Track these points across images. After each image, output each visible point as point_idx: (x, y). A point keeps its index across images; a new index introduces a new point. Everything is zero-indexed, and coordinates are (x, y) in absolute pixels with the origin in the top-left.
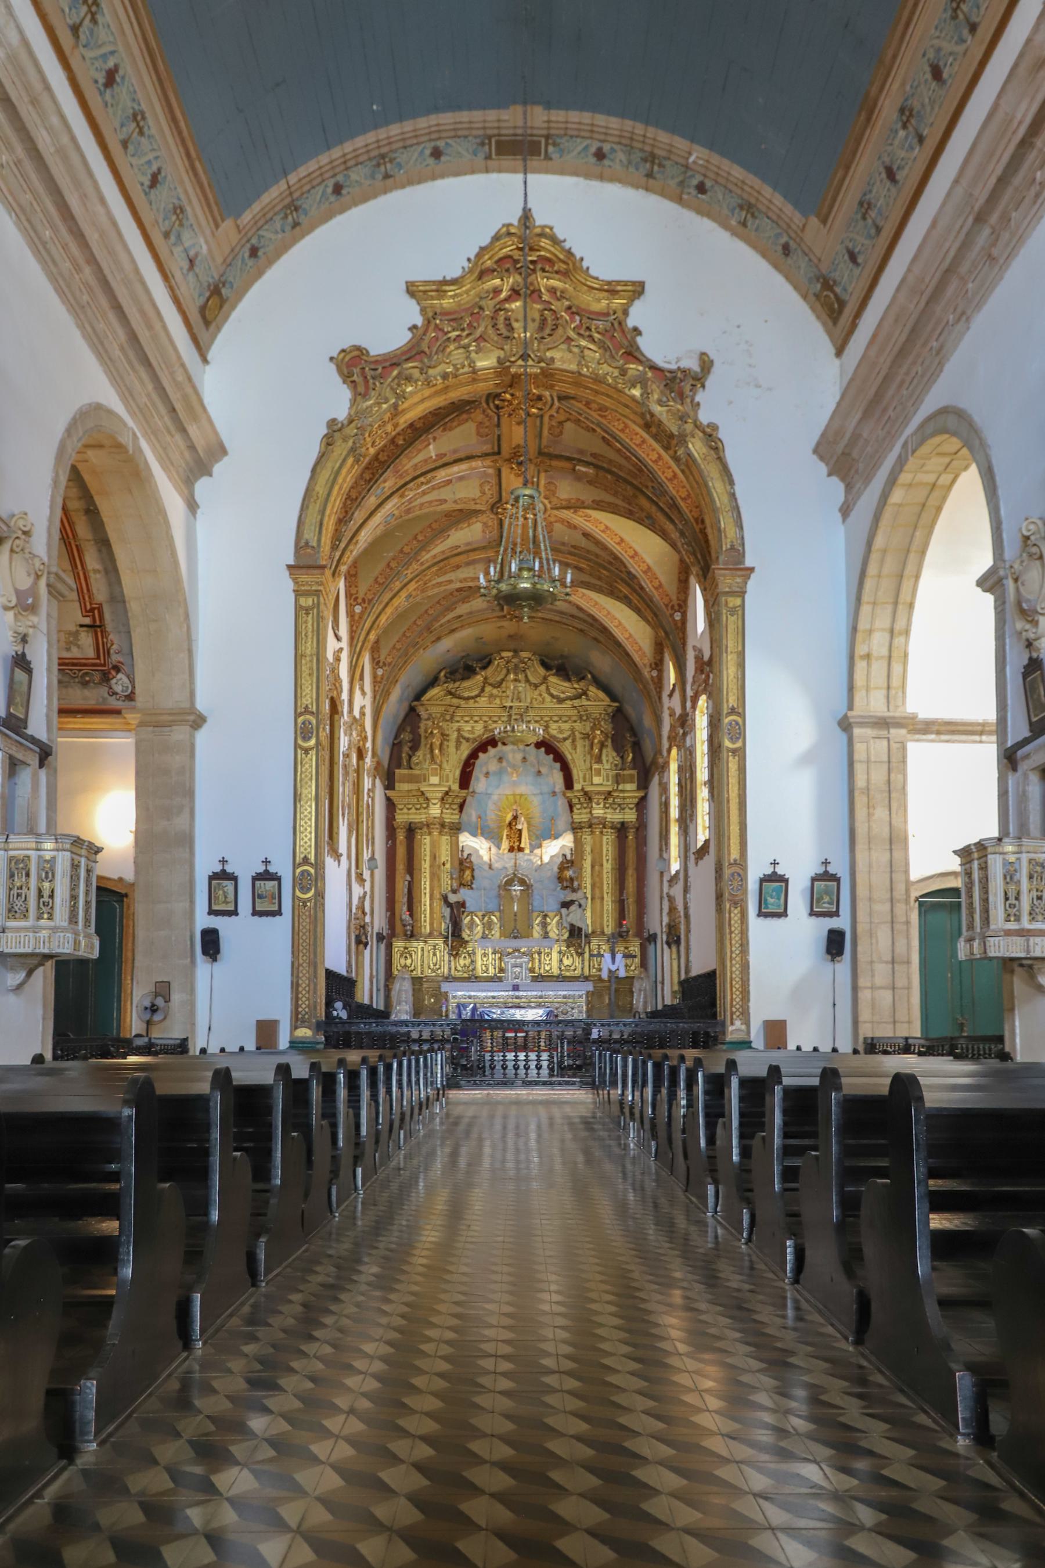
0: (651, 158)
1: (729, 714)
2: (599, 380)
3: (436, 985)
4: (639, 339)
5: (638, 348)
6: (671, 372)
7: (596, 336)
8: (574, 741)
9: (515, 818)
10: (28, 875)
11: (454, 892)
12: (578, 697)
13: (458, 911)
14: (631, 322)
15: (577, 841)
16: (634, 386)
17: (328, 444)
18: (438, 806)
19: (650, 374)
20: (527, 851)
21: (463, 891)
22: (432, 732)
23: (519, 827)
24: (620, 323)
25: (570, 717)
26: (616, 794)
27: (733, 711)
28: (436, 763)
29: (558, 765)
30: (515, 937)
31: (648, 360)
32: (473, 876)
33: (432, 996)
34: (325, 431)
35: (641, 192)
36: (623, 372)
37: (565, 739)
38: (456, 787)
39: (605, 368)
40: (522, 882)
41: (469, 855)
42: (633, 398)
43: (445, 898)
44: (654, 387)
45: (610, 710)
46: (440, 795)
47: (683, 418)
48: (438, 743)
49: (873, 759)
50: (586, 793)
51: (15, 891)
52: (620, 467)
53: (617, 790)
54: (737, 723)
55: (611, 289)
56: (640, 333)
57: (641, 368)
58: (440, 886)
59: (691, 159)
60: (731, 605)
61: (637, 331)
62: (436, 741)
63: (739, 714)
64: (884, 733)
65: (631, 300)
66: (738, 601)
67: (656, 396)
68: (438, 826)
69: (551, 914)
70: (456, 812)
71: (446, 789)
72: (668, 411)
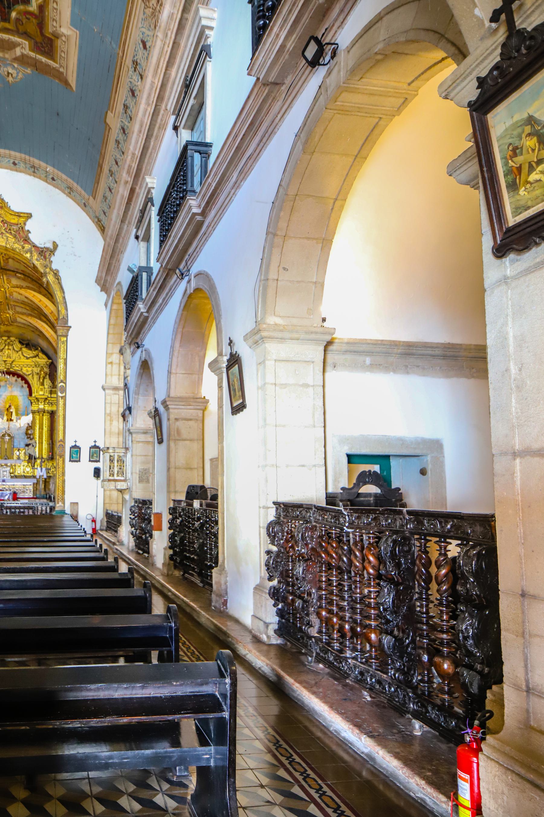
0: (33, 167)
1: (60, 383)
2: (13, 250)
4: (30, 235)
5: (29, 239)
6: (41, 248)
7: (13, 232)
8: (33, 375)
9: (10, 406)
12: (35, 357)
14: (27, 228)
15: (34, 418)
16: (27, 253)
19: (33, 249)
20: (15, 421)
23: (11, 410)
24: (22, 228)
25: (31, 365)
26: (49, 399)
27: (62, 381)
29: (26, 385)
30: (6, 459)
31: (33, 243)
35: (32, 177)
36: (23, 248)
37: (29, 375)
39: (16, 246)
40: (9, 435)
42: (27, 258)
44: (35, 254)
45: (48, 363)
47: (46, 267)
49: (113, 402)
50: (37, 398)
52: (33, 276)
53: (51, 397)
54: (63, 386)
55: (19, 215)
56: (30, 232)
57: (30, 246)
59: (48, 170)
60: (62, 340)
61: (29, 231)
63: (64, 383)
64: (117, 392)
65: (27, 220)
66: (65, 339)
67: (36, 257)
69: (21, 449)
72: (40, 263)
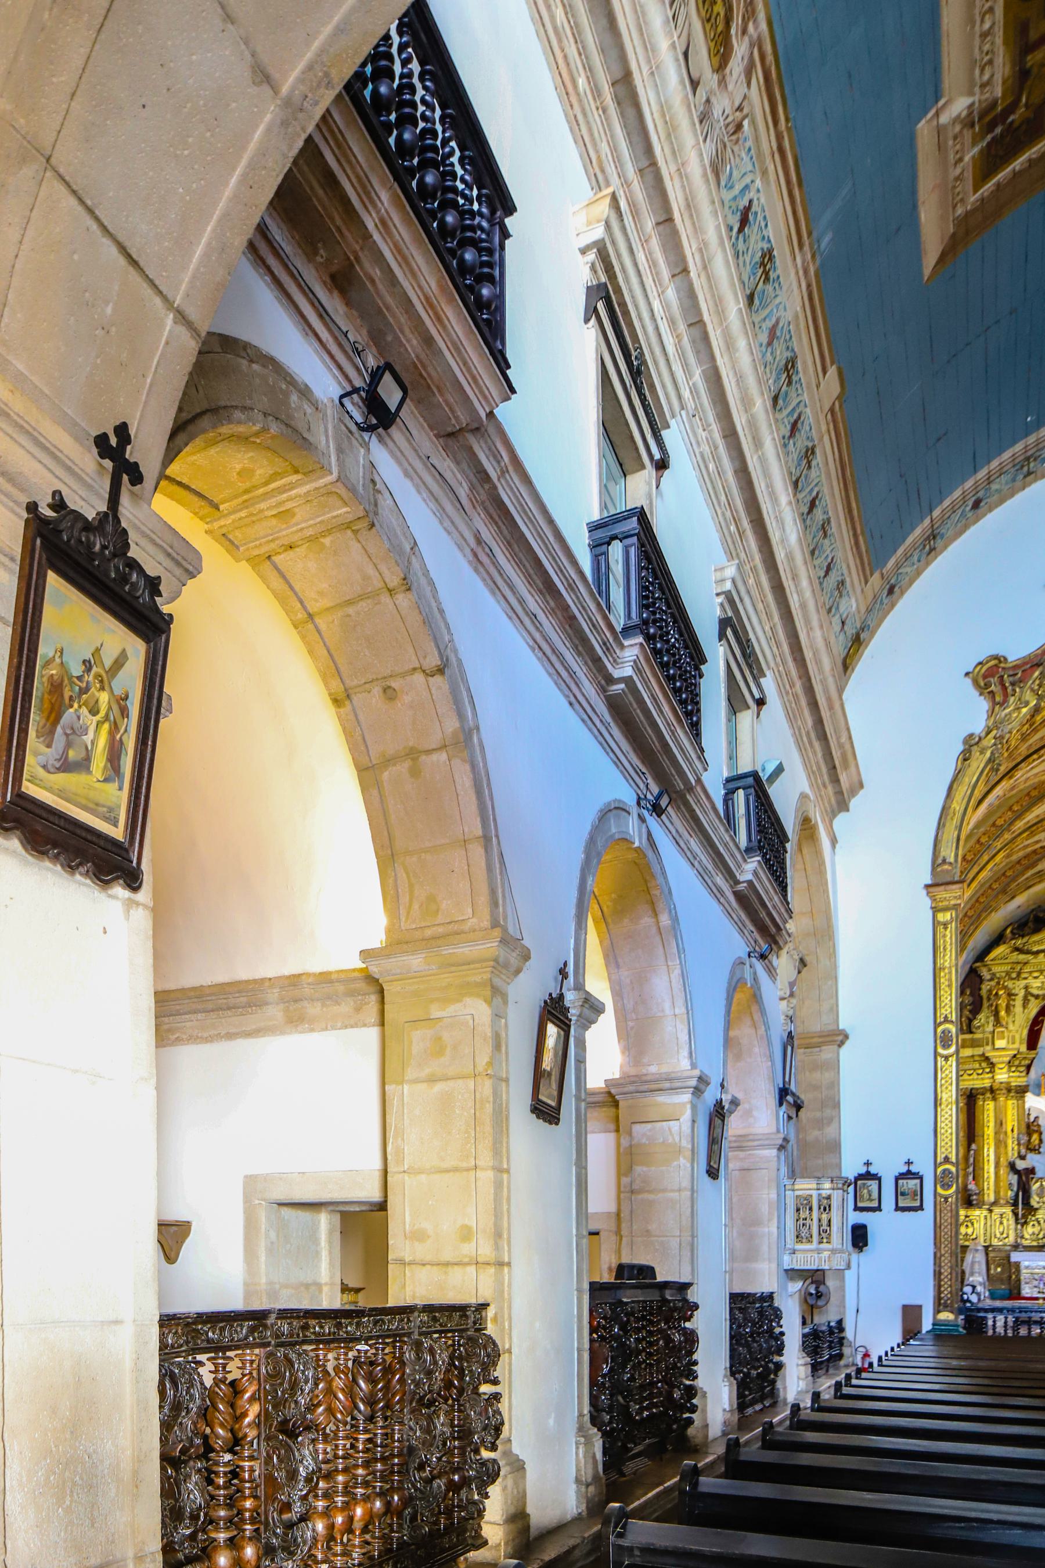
3: (1003, 1254)
10: (811, 1209)
11: (1022, 1158)
13: (1027, 1178)
17: (965, 760)
18: (1005, 1070)
21: (1030, 1156)
22: (997, 994)
28: (1002, 1026)
32: (1041, 1141)
33: (999, 1265)
34: (961, 748)
38: (1024, 1048)
41: (1037, 1118)
43: (1012, 1166)
46: (1007, 1059)
48: (1004, 1005)
51: (801, 1222)
58: (1006, 1153)
62: (1002, 1003)
68: (1004, 1091)
70: (1024, 1074)
71: (1015, 1052)
